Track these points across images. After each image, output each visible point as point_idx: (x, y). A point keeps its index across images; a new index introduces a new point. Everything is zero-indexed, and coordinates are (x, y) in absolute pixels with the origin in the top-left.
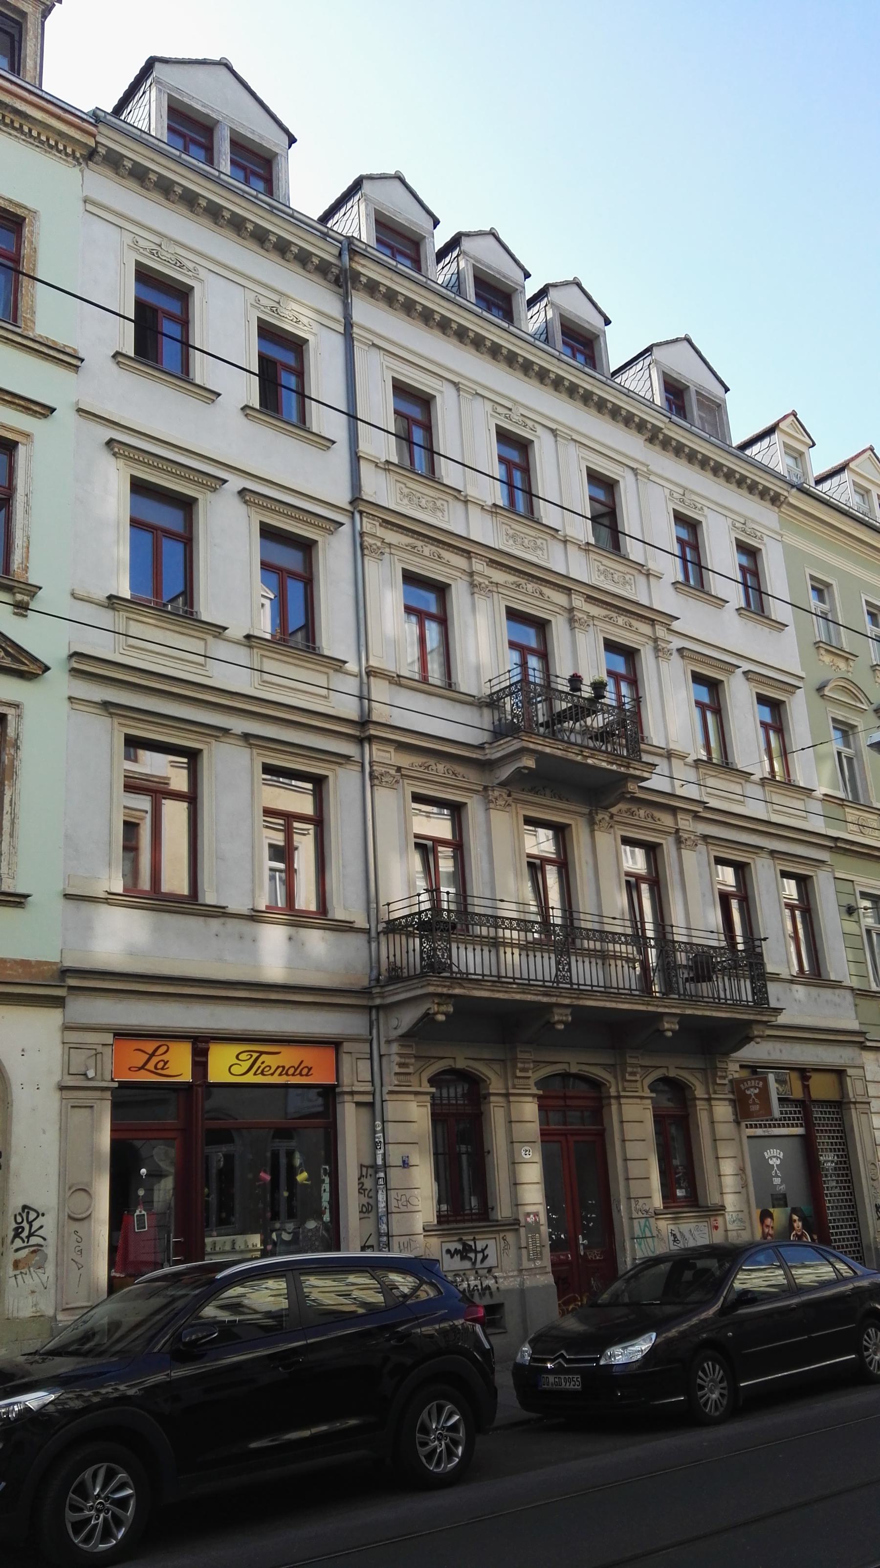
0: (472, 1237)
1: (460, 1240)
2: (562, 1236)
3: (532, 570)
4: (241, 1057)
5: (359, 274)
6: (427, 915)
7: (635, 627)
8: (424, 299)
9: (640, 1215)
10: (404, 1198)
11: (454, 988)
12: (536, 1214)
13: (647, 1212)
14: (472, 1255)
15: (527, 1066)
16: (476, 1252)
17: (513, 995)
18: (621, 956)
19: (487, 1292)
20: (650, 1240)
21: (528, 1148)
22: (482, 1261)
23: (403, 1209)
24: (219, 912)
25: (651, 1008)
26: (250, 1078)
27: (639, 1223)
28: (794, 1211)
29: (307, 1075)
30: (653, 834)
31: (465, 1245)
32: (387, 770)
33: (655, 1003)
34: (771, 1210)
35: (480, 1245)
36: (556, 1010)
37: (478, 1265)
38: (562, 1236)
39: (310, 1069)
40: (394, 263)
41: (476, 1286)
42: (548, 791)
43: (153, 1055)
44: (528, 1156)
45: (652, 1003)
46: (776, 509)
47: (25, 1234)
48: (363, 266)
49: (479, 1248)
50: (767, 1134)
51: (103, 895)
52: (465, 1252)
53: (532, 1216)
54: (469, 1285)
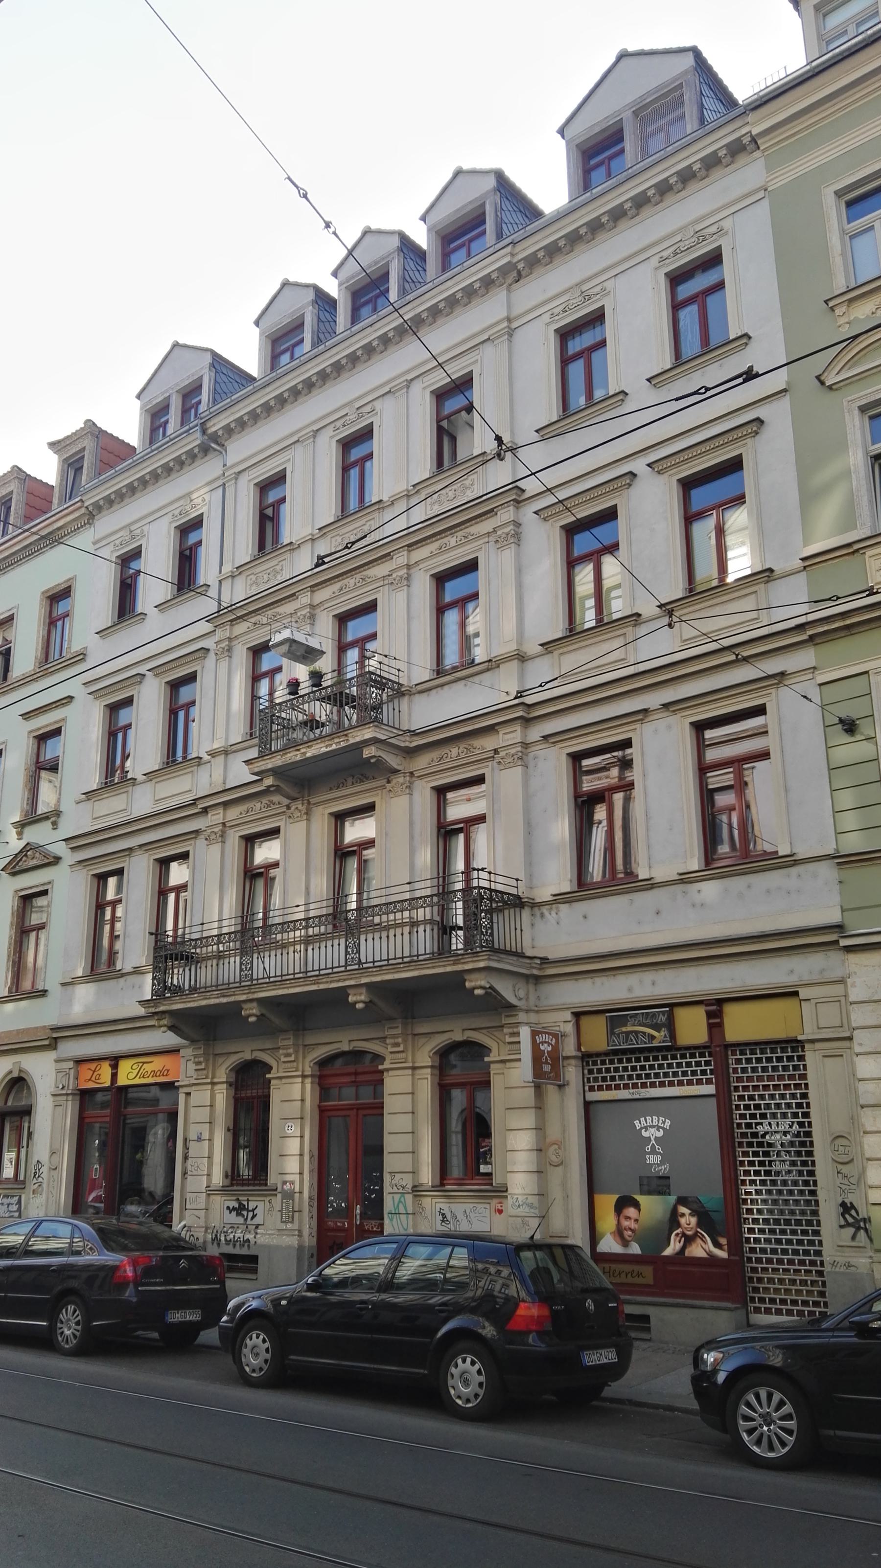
0: (246, 1198)
1: (238, 1200)
2: (343, 1205)
3: (364, 559)
4: (134, 1067)
5: (216, 432)
6: (224, 938)
7: (282, 612)
8: (268, 395)
9: (395, 1190)
10: (196, 1165)
11: (160, 1007)
12: (292, 1183)
13: (403, 1188)
14: (245, 1213)
15: (396, 1041)
16: (248, 1211)
17: (200, 1002)
18: (295, 941)
19: (246, 1244)
20: (403, 1217)
21: (290, 1124)
22: (252, 1218)
23: (195, 1173)
24: (650, 885)
25: (322, 987)
26: (138, 1081)
27: (393, 1197)
28: (682, 1201)
29: (166, 1075)
30: (444, 775)
31: (240, 1204)
32: (507, 752)
33: (324, 980)
34: (640, 1198)
35: (252, 1206)
36: (245, 1006)
37: (249, 1222)
38: (343, 1205)
39: (168, 1071)
40: (298, 361)
41: (239, 1238)
42: (350, 780)
43: (94, 1072)
44: (290, 1131)
45: (320, 981)
46: (757, 154)
47: (37, 1176)
48: (214, 425)
49: (250, 1208)
50: (637, 1097)
51: (132, 970)
52: (240, 1210)
53: (288, 1184)
54: (234, 1236)
